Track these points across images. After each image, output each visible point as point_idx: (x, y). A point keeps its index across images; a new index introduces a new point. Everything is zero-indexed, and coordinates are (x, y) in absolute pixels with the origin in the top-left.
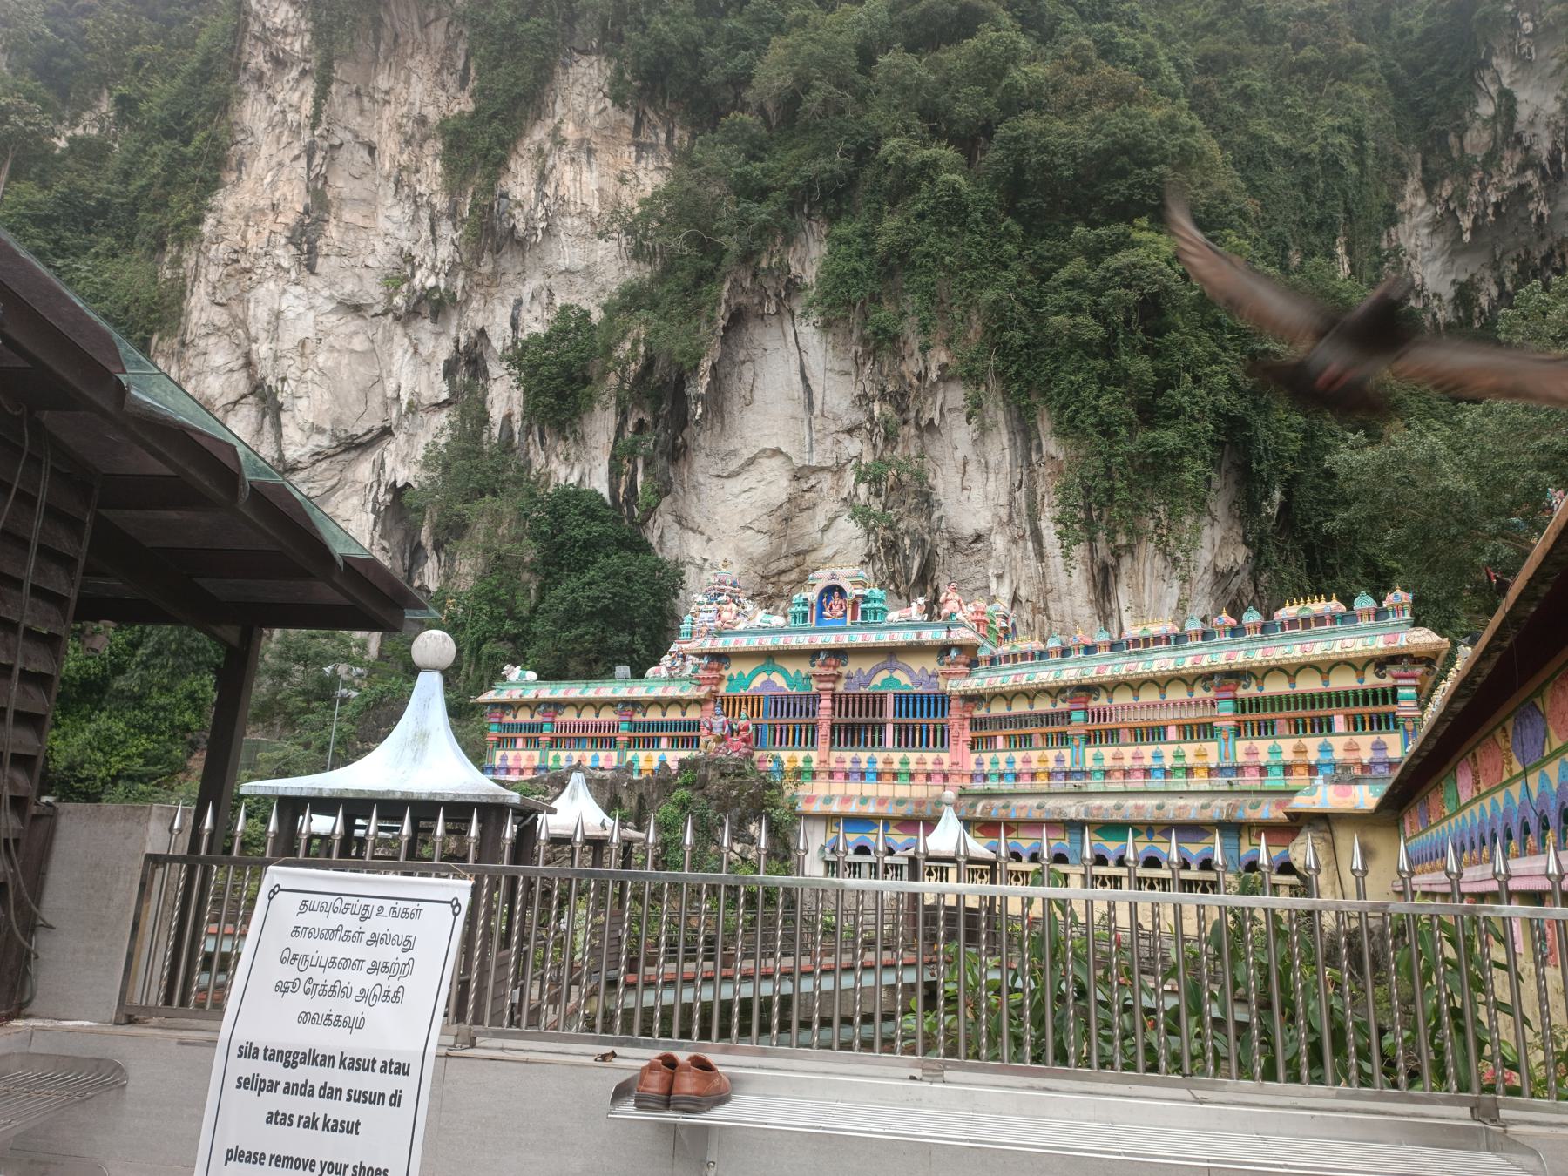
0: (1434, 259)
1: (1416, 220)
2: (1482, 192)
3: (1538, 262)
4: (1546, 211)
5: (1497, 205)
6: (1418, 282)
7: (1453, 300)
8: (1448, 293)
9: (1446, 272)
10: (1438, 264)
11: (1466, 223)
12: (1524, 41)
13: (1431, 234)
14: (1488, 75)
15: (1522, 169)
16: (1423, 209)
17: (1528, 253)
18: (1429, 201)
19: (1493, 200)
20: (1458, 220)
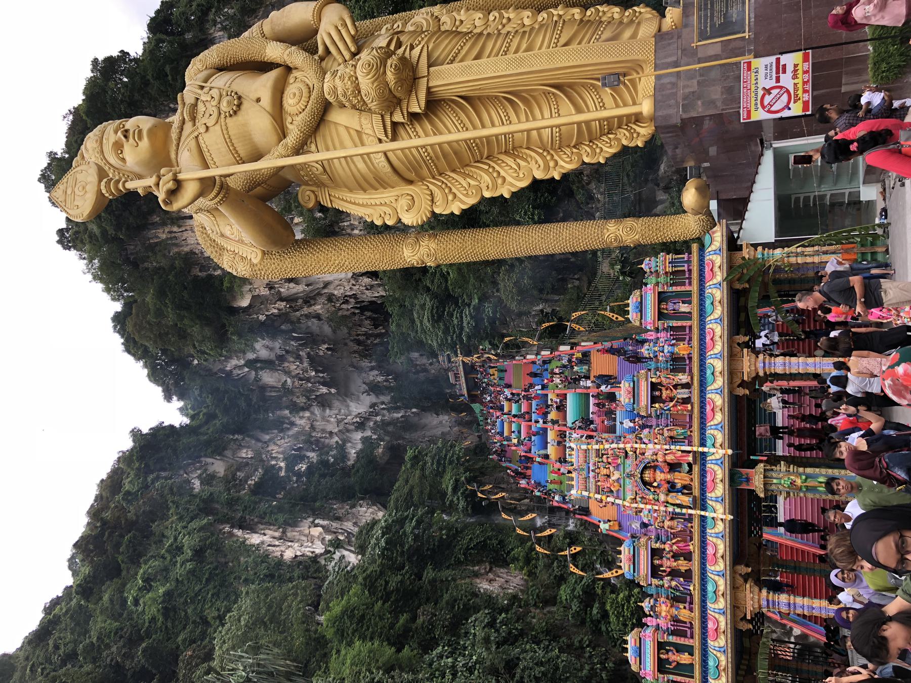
0: (348, 406)
1: (319, 417)
2: (308, 380)
5: (317, 371)
6: (358, 420)
7: (377, 396)
8: (372, 399)
10: (351, 404)
11: (324, 390)
13: (330, 407)
15: (299, 358)
16: (312, 413)
17: (355, 352)
19: (314, 373)
20: (322, 395)
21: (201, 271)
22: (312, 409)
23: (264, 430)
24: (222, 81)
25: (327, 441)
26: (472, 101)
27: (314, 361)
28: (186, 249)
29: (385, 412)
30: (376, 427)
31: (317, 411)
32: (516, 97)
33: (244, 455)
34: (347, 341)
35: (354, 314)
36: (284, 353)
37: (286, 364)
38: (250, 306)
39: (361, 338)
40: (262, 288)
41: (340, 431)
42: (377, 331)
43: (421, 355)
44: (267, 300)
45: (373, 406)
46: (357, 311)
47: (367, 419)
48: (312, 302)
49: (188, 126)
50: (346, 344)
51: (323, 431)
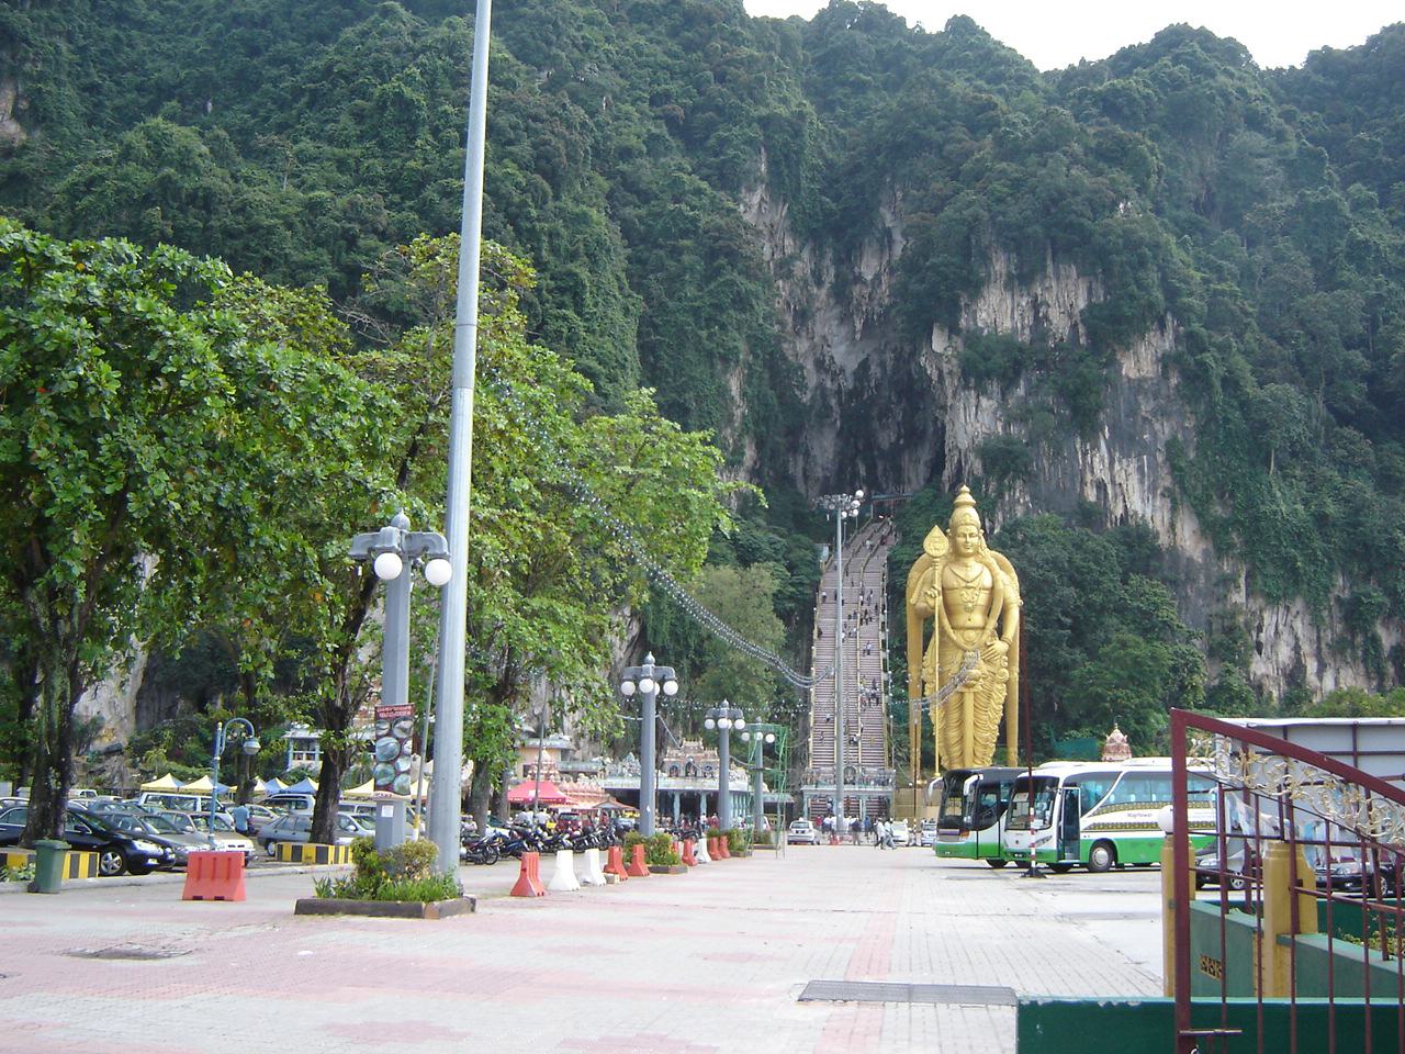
0: (841, 343)
1: (828, 315)
11: (859, 326)
23: (813, 250)
24: (982, 598)
25: (804, 334)
26: (961, 706)
28: (985, 294)
29: (835, 387)
30: (821, 386)
31: (836, 311)
32: (961, 722)
33: (786, 243)
43: (898, 424)
45: (842, 370)
47: (827, 371)
49: (964, 584)
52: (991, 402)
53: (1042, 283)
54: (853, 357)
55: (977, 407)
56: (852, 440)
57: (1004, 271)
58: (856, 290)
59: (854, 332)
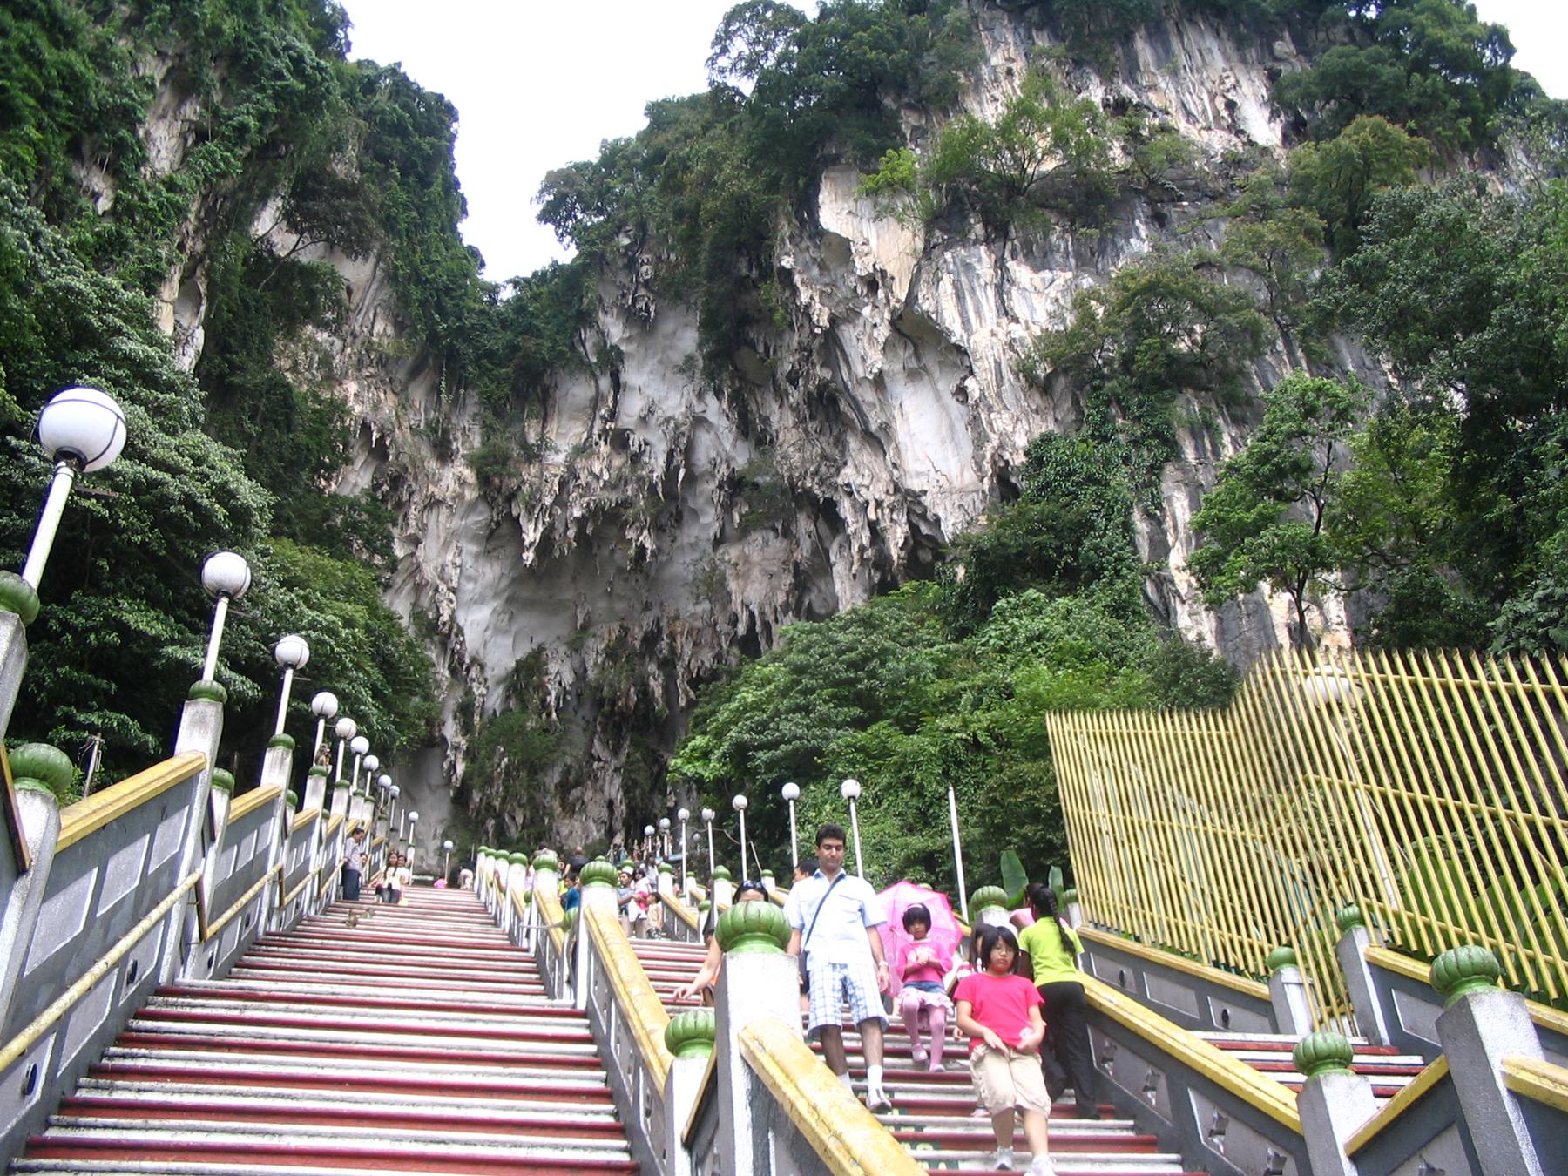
0: (480, 600)
1: (456, 523)
2: (561, 501)
3: (637, 644)
4: (649, 545)
5: (581, 522)
6: (445, 618)
9: (498, 631)
11: (532, 534)
12: (642, 292)
14: (590, 338)
16: (472, 507)
17: (625, 630)
18: (484, 497)
19: (577, 513)
20: (518, 530)
21: (914, 129)
22: (482, 507)
23: (435, 389)
27: (606, 521)
29: (459, 694)
31: (481, 517)
33: (379, 327)
34: (655, 612)
35: (734, 622)
36: (634, 449)
37: (604, 449)
38: (819, 234)
39: (664, 644)
40: (870, 260)
41: (418, 567)
42: (681, 684)
43: (610, 804)
44: (833, 284)
46: (741, 629)
48: (812, 426)
50: (647, 607)
51: (424, 528)
52: (1047, 274)
53: (1131, 79)
54: (509, 641)
55: (999, 290)
56: (491, 824)
57: (1019, 66)
58: (530, 472)
59: (521, 547)
